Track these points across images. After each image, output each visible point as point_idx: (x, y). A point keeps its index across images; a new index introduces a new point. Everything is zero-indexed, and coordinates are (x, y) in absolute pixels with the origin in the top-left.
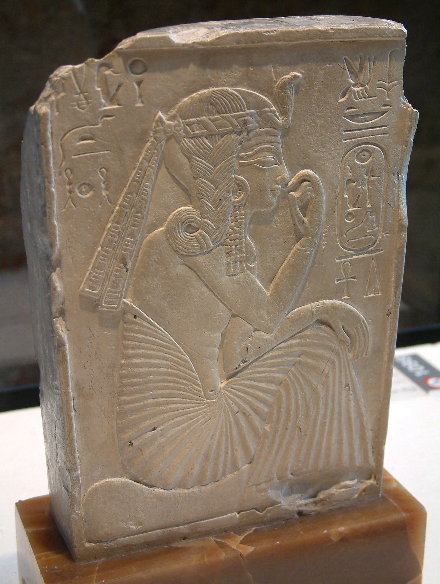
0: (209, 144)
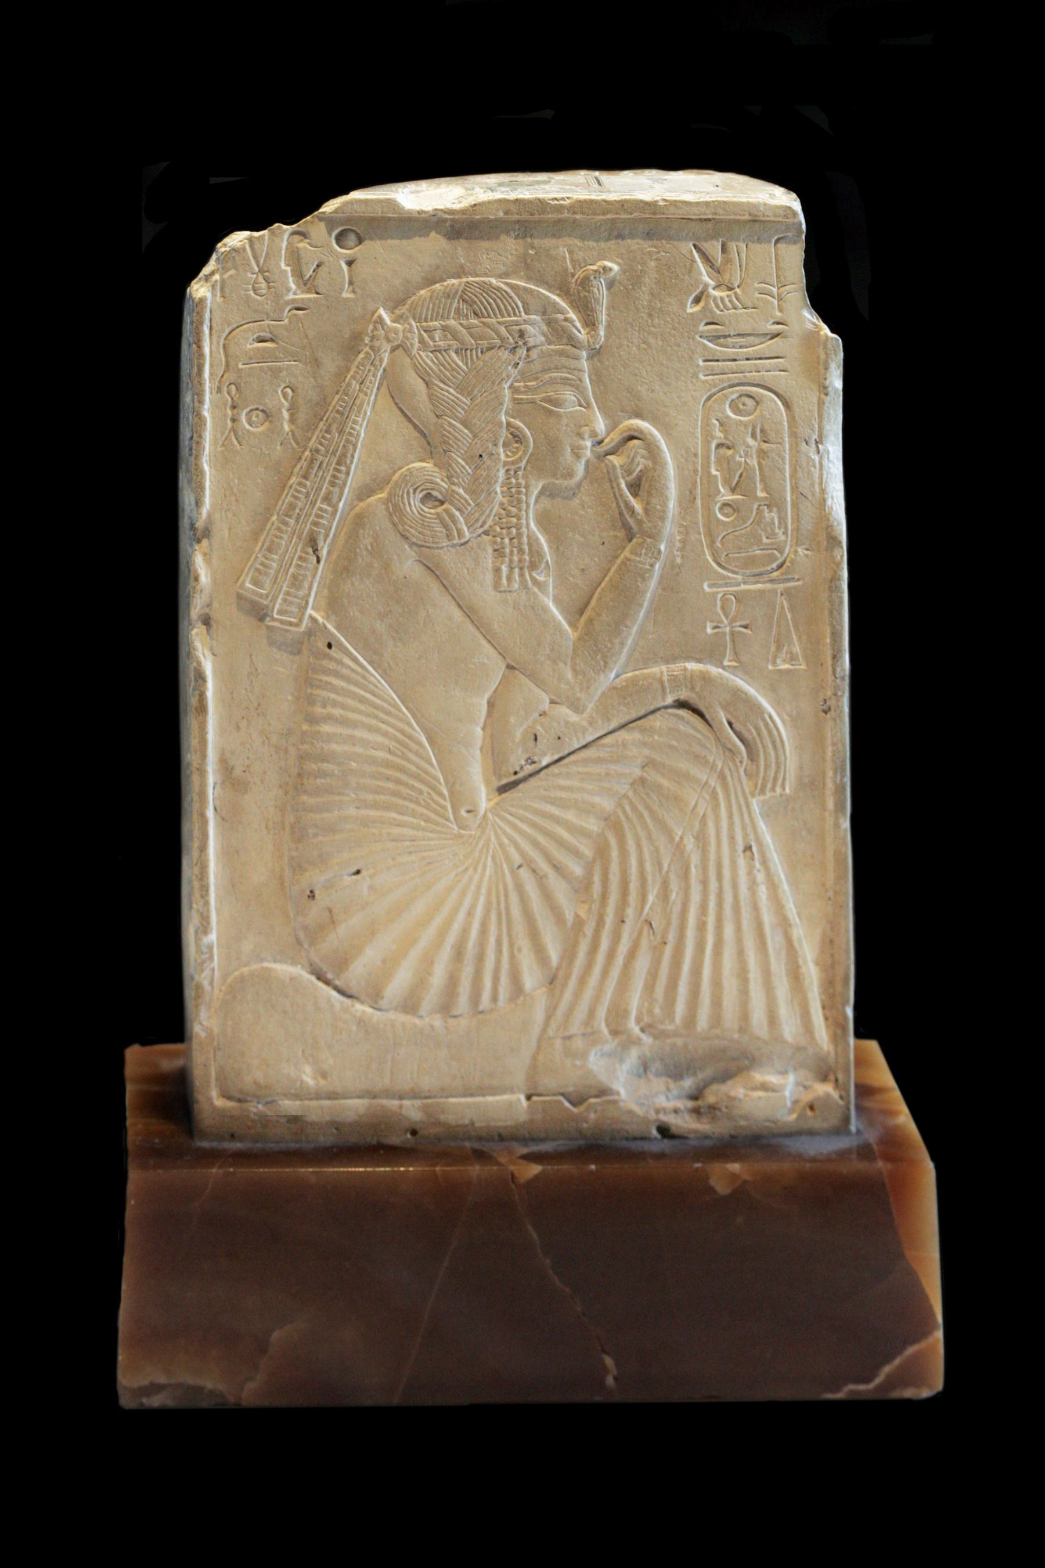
0: (461, 364)
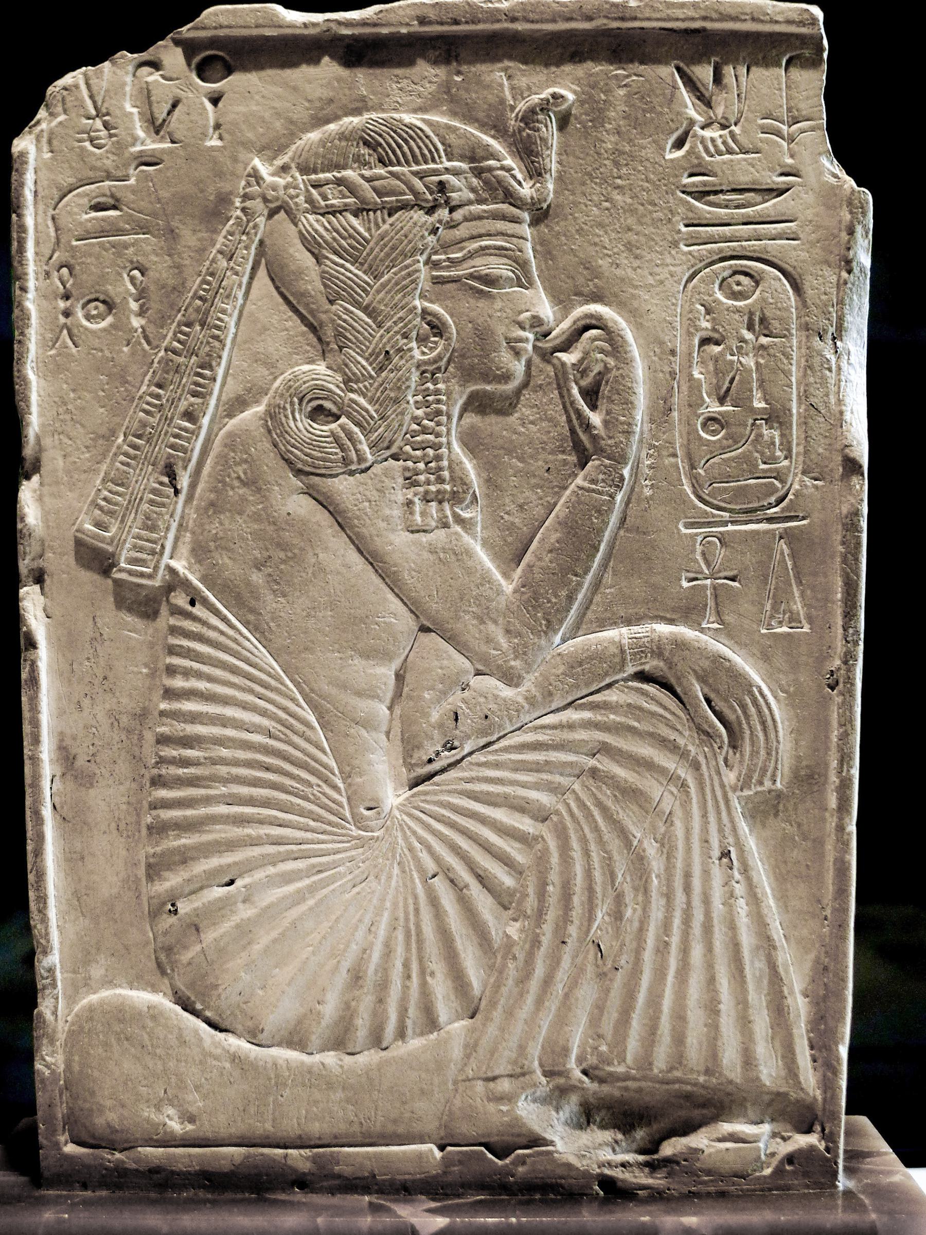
0: (361, 230)
